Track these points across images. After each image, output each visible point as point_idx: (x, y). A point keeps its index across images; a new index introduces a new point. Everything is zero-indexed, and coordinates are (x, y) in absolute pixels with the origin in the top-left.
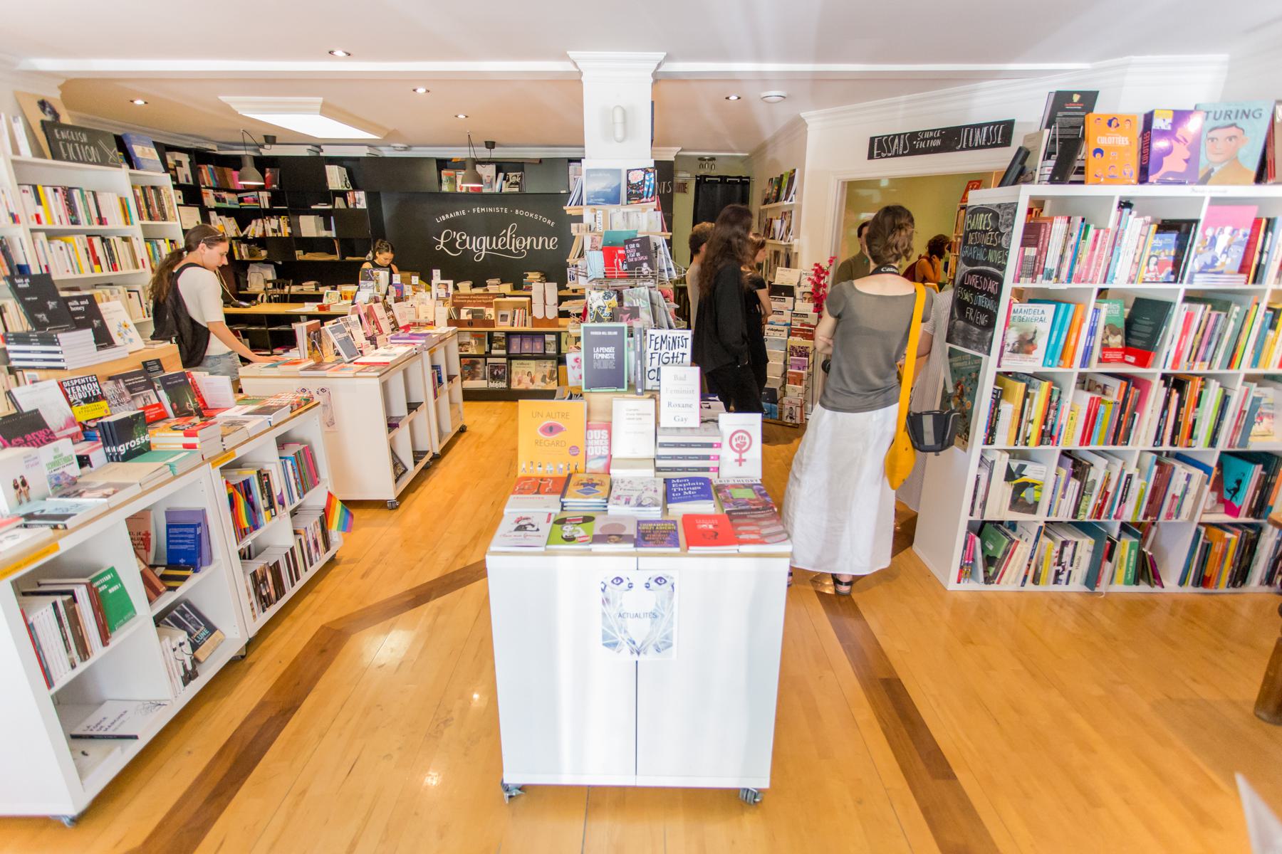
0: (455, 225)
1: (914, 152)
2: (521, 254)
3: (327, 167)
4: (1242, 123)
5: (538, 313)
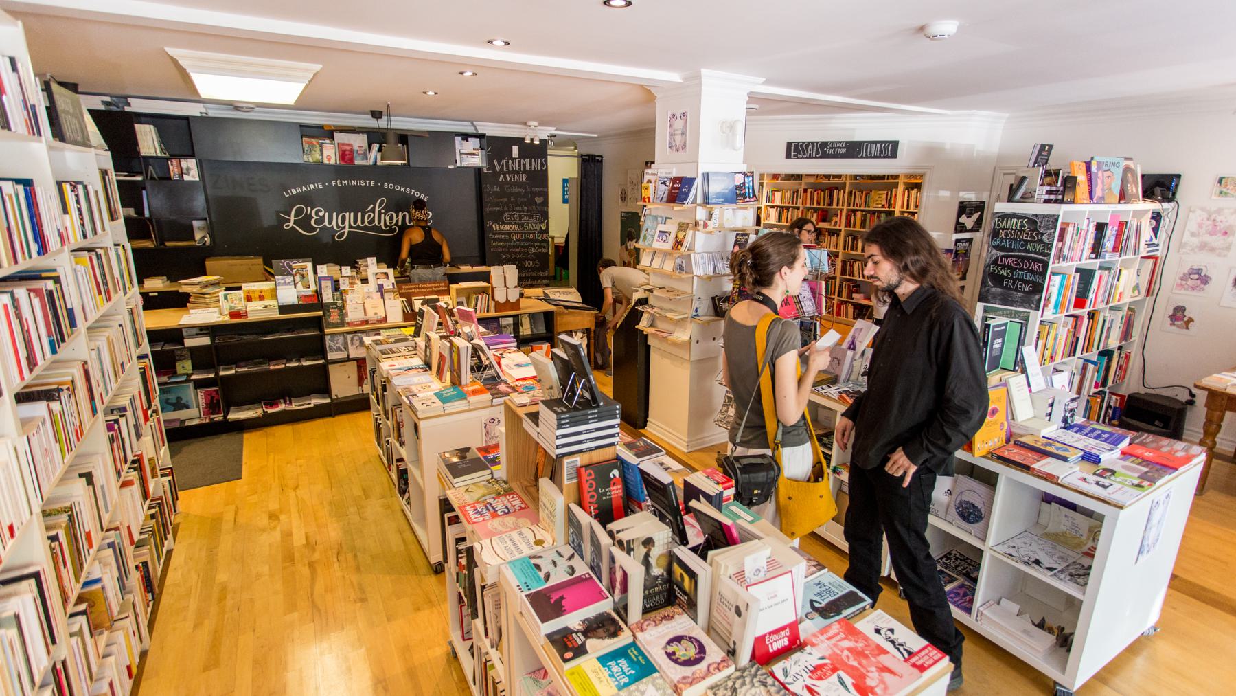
0: (306, 199)
1: (825, 156)
2: (393, 231)
3: (137, 126)
4: (1112, 169)
5: (500, 297)
